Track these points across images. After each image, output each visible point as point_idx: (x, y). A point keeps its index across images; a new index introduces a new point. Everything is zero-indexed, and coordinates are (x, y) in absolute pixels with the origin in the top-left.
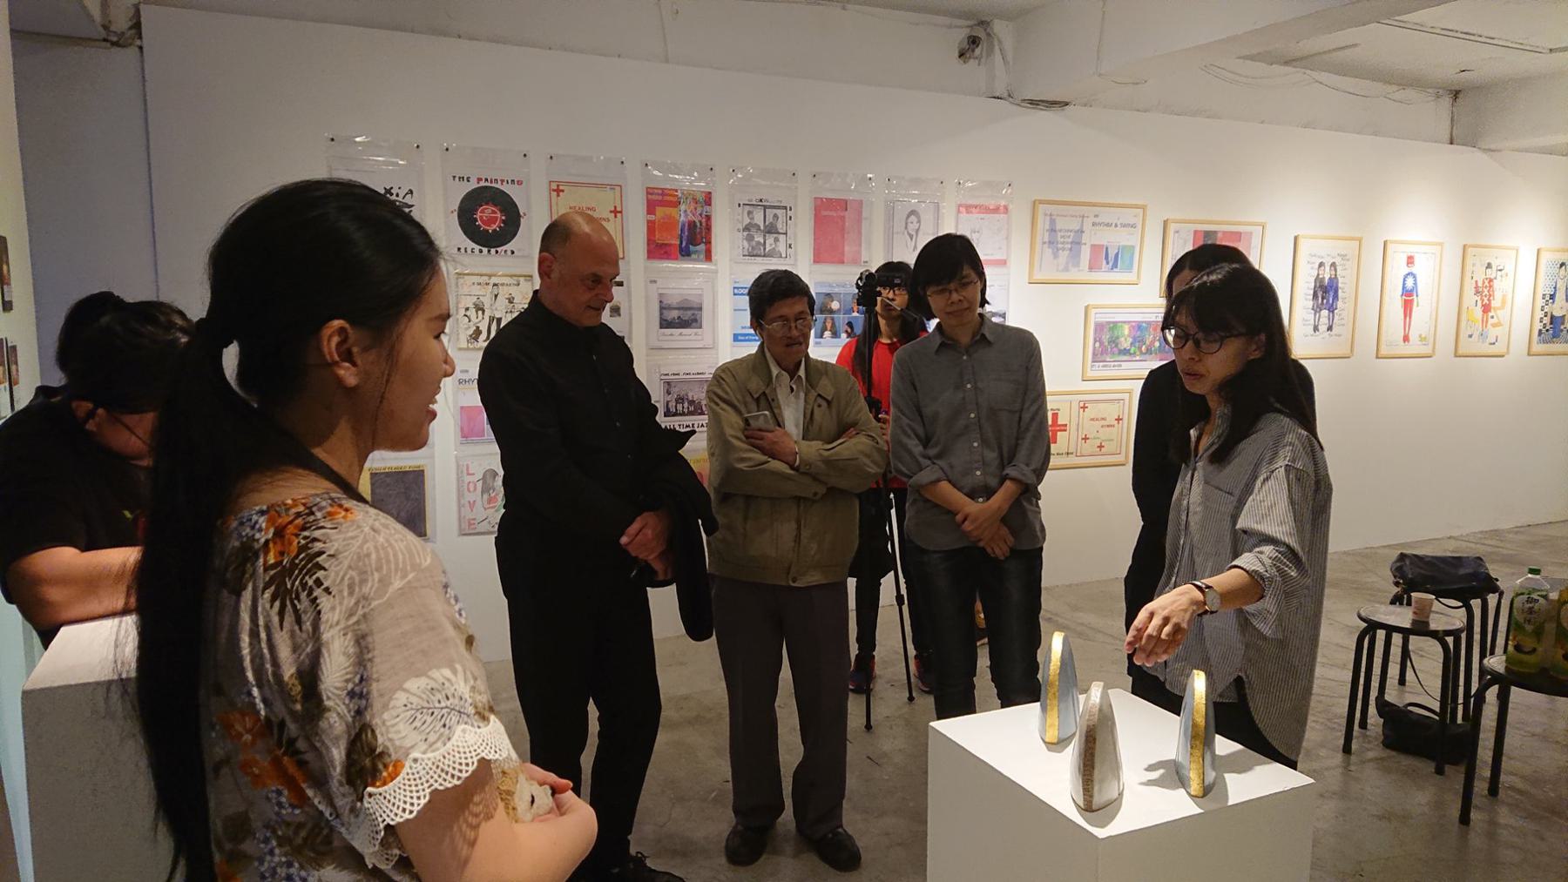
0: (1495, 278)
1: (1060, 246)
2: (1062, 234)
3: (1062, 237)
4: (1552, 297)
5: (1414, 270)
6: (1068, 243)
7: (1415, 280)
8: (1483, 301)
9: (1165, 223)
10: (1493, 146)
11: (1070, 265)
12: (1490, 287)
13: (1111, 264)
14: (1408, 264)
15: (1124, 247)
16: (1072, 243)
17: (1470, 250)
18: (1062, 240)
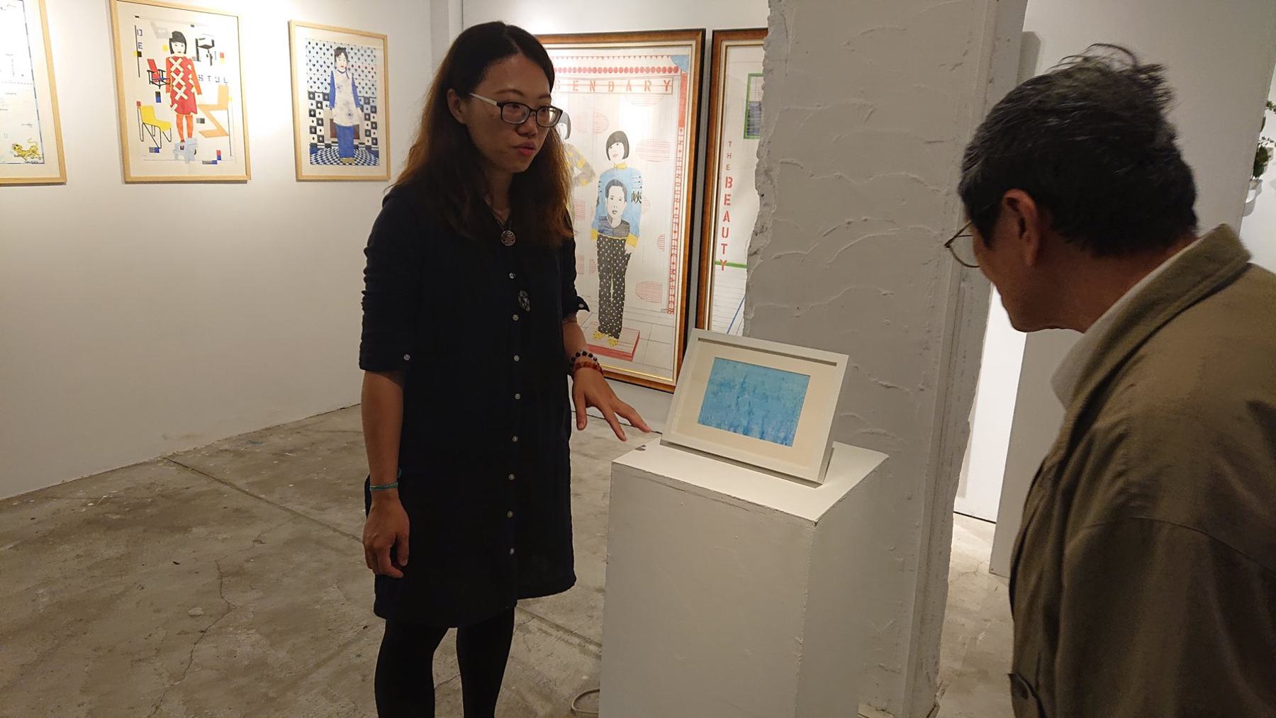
0: (198, 60)
4: (330, 97)
8: (174, 94)
12: (187, 72)
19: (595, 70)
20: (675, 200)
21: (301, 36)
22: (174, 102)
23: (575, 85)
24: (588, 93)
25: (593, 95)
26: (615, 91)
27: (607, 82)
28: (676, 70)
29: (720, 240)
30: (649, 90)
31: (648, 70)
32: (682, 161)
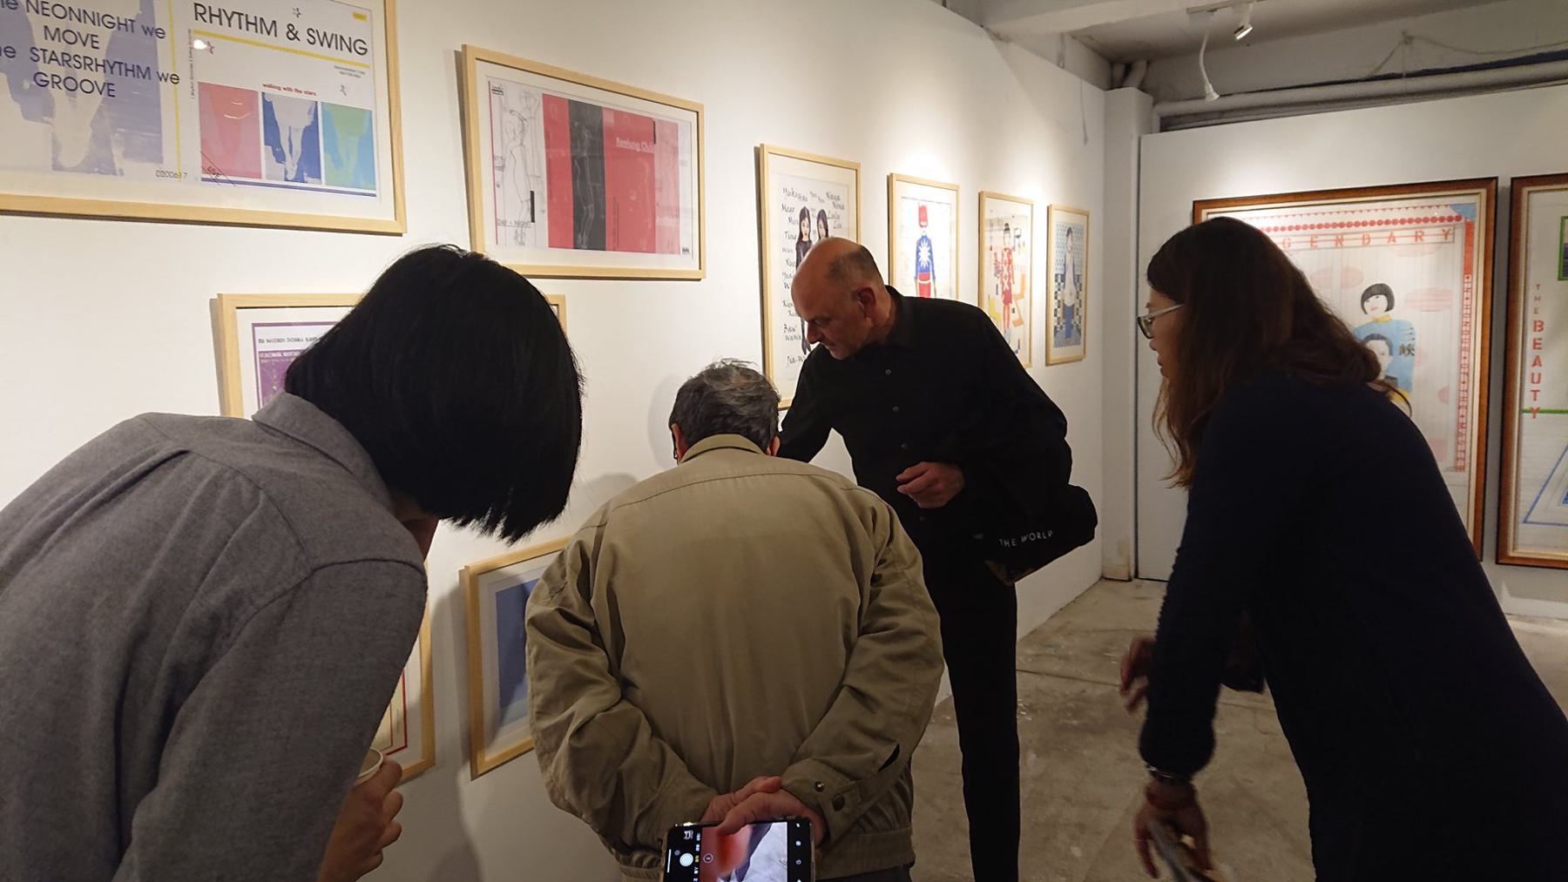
0: (1014, 248)
1: (50, 69)
2: (53, 23)
3: (58, 35)
5: (929, 232)
6: (88, 63)
7: (930, 251)
8: (1003, 283)
9: (460, 60)
10: (1000, 27)
11: (117, 152)
12: (1010, 262)
13: (291, 165)
14: (920, 220)
15: (331, 109)
16: (109, 66)
17: (989, 203)
18: (59, 47)
19: (1342, 225)
20: (1461, 349)
21: (1056, 216)
22: (1003, 293)
23: (1312, 242)
24: (1334, 248)
25: (1340, 250)
26: (1371, 244)
27: (1360, 236)
28: (1458, 218)
29: (1528, 386)
30: (1422, 240)
31: (1418, 221)
32: (1471, 308)
